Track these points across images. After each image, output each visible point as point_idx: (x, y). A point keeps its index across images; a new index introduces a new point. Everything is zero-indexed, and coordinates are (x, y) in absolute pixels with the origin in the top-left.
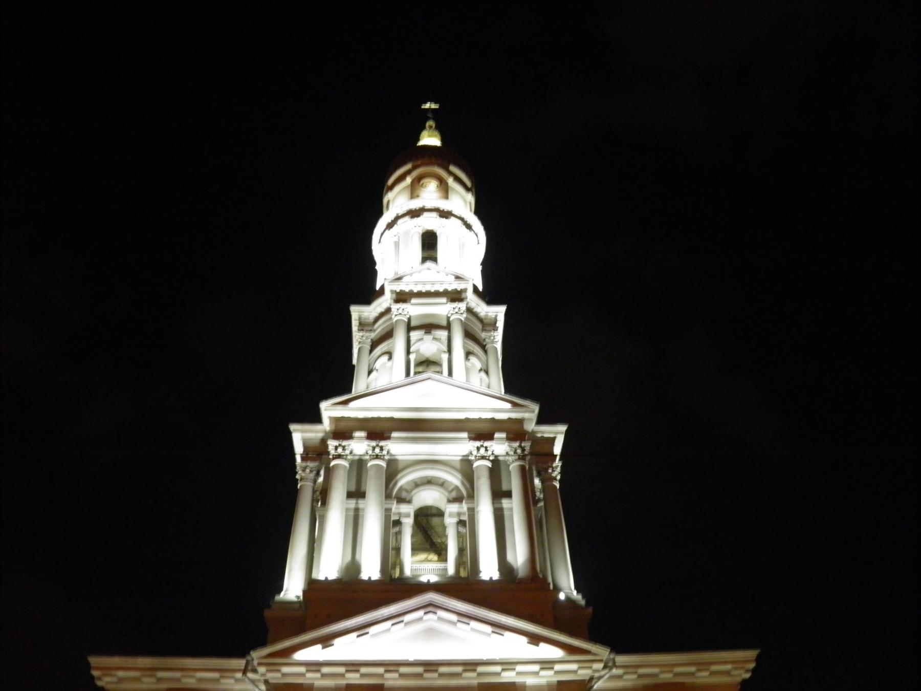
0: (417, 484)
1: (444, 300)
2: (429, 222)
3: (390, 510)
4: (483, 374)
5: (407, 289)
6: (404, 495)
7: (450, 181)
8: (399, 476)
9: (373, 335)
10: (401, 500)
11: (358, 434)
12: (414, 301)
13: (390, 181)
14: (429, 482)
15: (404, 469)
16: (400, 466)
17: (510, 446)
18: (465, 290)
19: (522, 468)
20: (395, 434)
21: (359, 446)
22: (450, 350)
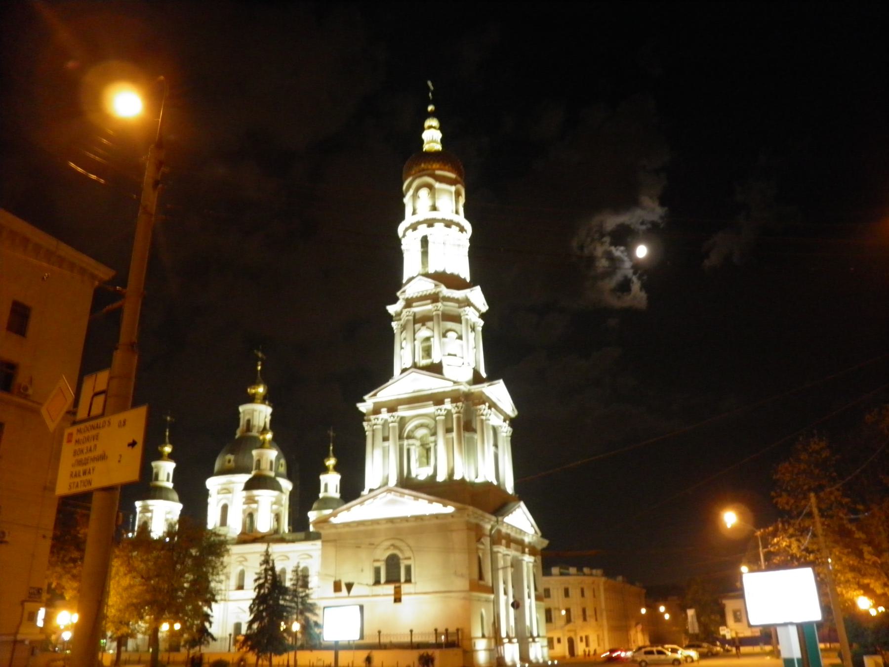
0: (417, 427)
1: (429, 301)
2: (423, 230)
3: (403, 445)
5: (410, 297)
6: (411, 434)
7: (437, 185)
8: (407, 425)
9: (402, 322)
10: (409, 437)
12: (414, 304)
13: (404, 187)
14: (422, 426)
15: (408, 421)
16: (407, 420)
17: (452, 406)
18: (441, 292)
19: (458, 418)
20: (399, 407)
21: (384, 415)
22: (433, 337)
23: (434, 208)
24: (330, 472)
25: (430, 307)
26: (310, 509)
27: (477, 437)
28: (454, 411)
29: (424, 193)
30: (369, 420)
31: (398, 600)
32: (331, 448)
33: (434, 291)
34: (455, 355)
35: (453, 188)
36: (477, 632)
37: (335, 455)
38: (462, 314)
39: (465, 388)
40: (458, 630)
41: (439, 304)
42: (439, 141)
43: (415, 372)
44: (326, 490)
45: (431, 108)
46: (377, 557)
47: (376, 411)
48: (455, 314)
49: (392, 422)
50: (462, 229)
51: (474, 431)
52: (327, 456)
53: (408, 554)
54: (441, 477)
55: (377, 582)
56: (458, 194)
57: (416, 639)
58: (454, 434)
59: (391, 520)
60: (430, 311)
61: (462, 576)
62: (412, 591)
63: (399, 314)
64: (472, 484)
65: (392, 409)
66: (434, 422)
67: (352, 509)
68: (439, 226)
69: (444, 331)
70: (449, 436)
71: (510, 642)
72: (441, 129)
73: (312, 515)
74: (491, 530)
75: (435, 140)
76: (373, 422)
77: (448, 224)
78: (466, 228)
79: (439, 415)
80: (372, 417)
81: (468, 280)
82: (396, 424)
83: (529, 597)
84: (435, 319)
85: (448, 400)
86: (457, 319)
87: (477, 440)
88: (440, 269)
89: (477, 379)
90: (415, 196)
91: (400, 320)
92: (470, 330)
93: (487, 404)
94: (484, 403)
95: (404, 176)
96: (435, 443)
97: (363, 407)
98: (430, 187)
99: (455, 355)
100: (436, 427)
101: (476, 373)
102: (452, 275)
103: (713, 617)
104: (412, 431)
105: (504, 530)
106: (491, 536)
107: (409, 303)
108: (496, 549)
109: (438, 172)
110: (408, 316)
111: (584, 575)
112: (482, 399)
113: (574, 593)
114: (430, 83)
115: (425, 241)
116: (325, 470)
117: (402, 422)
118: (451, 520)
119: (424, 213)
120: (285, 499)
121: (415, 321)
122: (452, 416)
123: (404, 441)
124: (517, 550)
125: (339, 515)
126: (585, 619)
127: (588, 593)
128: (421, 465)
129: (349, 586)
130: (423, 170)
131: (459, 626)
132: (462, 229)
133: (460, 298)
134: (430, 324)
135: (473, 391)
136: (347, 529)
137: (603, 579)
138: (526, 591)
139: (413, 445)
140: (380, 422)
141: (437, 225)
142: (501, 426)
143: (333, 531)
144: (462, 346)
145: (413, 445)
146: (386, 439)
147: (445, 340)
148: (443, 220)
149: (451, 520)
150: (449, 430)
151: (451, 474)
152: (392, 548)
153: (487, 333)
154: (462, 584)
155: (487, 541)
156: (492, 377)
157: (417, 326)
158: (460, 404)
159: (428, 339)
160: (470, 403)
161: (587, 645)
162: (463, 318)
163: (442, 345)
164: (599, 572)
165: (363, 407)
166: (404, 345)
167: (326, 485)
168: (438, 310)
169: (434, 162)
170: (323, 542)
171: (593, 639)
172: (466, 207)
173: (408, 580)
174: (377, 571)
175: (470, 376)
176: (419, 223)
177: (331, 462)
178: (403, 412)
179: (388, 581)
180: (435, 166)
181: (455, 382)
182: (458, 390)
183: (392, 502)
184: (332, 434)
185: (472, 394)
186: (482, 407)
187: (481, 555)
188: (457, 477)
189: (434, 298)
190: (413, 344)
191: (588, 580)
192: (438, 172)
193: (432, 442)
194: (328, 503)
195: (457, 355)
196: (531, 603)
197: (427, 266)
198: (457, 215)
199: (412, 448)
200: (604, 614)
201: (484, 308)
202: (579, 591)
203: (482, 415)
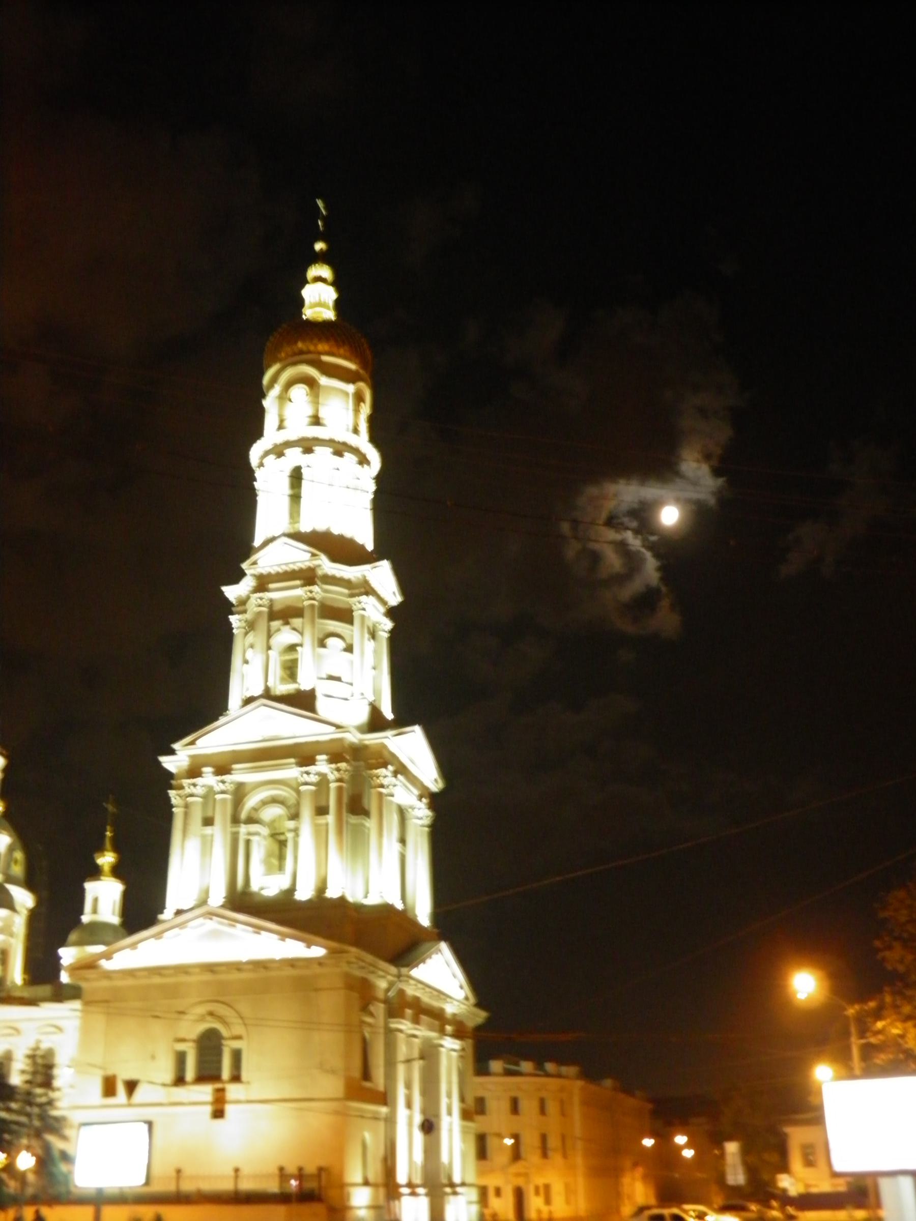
0: (265, 803)
1: (298, 582)
2: (294, 457)
4: (347, 654)
5: (264, 571)
7: (324, 381)
8: (245, 799)
9: (248, 616)
10: (251, 820)
11: (205, 770)
12: (272, 586)
13: (266, 379)
14: (274, 801)
16: (247, 788)
19: (340, 789)
20: (235, 766)
21: (208, 779)
23: (316, 421)
24: (102, 878)
25: (300, 592)
26: (63, 943)
27: (371, 824)
28: (331, 777)
29: (299, 392)
30: (181, 787)
31: (218, 1114)
32: (108, 834)
33: (308, 564)
34: (338, 679)
35: (351, 388)
36: (354, 1174)
37: (116, 849)
38: (354, 608)
39: (353, 737)
40: (321, 1170)
41: (315, 588)
42: (331, 304)
43: (265, 705)
44: (95, 911)
45: (319, 246)
46: (182, 1035)
47: (194, 772)
48: (341, 605)
49: (223, 792)
50: (363, 460)
51: (366, 813)
52: (101, 849)
53: (238, 1030)
54: (304, 893)
55: (180, 1080)
56: (359, 398)
57: (247, 1185)
58: (331, 819)
59: (211, 968)
60: (299, 598)
61: (333, 1072)
62: (242, 1097)
63: (243, 602)
64: (359, 908)
65: (222, 769)
66: (294, 794)
67: (140, 945)
68: (323, 453)
69: (321, 636)
70: (322, 820)
71: (413, 1194)
72: (336, 283)
73: (68, 955)
74: (388, 990)
75: (325, 302)
76: (188, 791)
77: (340, 449)
78: (369, 457)
79: (306, 784)
80: (186, 782)
81: (370, 546)
82: (228, 796)
83: (450, 1113)
84: (307, 613)
85: (322, 758)
86: (345, 615)
87: (369, 829)
88: (321, 527)
89: (376, 723)
90: (283, 398)
91: (245, 612)
92: (367, 636)
93: (390, 768)
94: (385, 765)
95: (265, 362)
96: (296, 831)
97: (169, 763)
98: (311, 383)
99: (338, 679)
100: (298, 805)
101: (375, 712)
102: (341, 538)
103: (766, 1156)
104: (255, 809)
105: (411, 991)
106: (386, 1001)
107: (263, 583)
108: (395, 1024)
109: (326, 358)
110: (260, 606)
111: (548, 1075)
112: (384, 758)
113: (528, 1106)
114: (320, 203)
115: (296, 476)
116: (95, 872)
117: (240, 793)
118: (318, 970)
119: (298, 427)
120: (19, 924)
121: (273, 615)
122: (328, 789)
123: (239, 826)
124: (431, 1029)
125: (115, 956)
126: (545, 1154)
127: (552, 1107)
128: (269, 871)
129: (131, 1086)
130: (301, 352)
131: (323, 1163)
132: (363, 460)
133: (353, 579)
134: (297, 622)
135: (367, 742)
136: (130, 982)
137: (580, 1083)
138: (444, 1101)
139: (257, 834)
140: (199, 790)
141: (317, 449)
142: (413, 808)
143: (105, 983)
144: (352, 663)
145: (257, 834)
146: (208, 822)
147: (322, 650)
148: (330, 443)
149: (318, 970)
150: (321, 811)
151: (322, 889)
152: (209, 1018)
153: (396, 641)
154: (333, 1086)
155: (379, 1009)
156: (402, 720)
157: (276, 624)
158: (343, 765)
159: (292, 648)
160: (362, 763)
161: (548, 1201)
162: (355, 614)
163: (318, 659)
164: (572, 1070)
165: (169, 763)
166: (250, 654)
167: (96, 900)
168: (314, 599)
169: (320, 340)
170: (87, 1003)
171: (558, 1189)
172: (373, 421)
173: (236, 1078)
174: (181, 1059)
175: (363, 716)
176: (288, 444)
177: (107, 859)
178: (241, 775)
179: (201, 1079)
180: (321, 347)
181: (338, 727)
182: (341, 740)
183: (214, 934)
184: (111, 808)
185: (366, 747)
186: (382, 771)
187: (367, 1035)
188: (332, 893)
189: (308, 577)
190: (264, 657)
191: (553, 1083)
192: (326, 358)
193: (290, 830)
194: (97, 933)
195: (343, 679)
196: (451, 1124)
197: (298, 522)
198: (355, 436)
199: (254, 839)
200: (580, 1145)
201: (395, 598)
202: (535, 1104)
203: (382, 786)
